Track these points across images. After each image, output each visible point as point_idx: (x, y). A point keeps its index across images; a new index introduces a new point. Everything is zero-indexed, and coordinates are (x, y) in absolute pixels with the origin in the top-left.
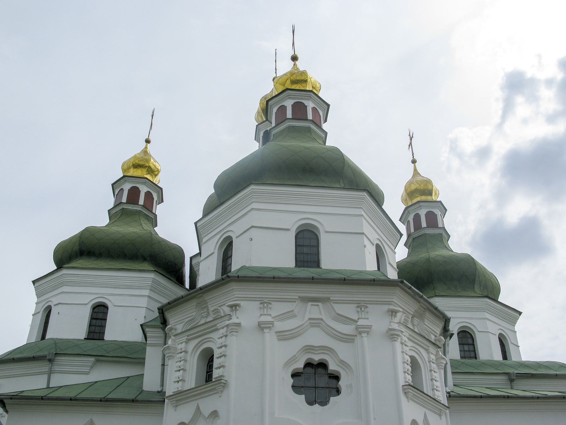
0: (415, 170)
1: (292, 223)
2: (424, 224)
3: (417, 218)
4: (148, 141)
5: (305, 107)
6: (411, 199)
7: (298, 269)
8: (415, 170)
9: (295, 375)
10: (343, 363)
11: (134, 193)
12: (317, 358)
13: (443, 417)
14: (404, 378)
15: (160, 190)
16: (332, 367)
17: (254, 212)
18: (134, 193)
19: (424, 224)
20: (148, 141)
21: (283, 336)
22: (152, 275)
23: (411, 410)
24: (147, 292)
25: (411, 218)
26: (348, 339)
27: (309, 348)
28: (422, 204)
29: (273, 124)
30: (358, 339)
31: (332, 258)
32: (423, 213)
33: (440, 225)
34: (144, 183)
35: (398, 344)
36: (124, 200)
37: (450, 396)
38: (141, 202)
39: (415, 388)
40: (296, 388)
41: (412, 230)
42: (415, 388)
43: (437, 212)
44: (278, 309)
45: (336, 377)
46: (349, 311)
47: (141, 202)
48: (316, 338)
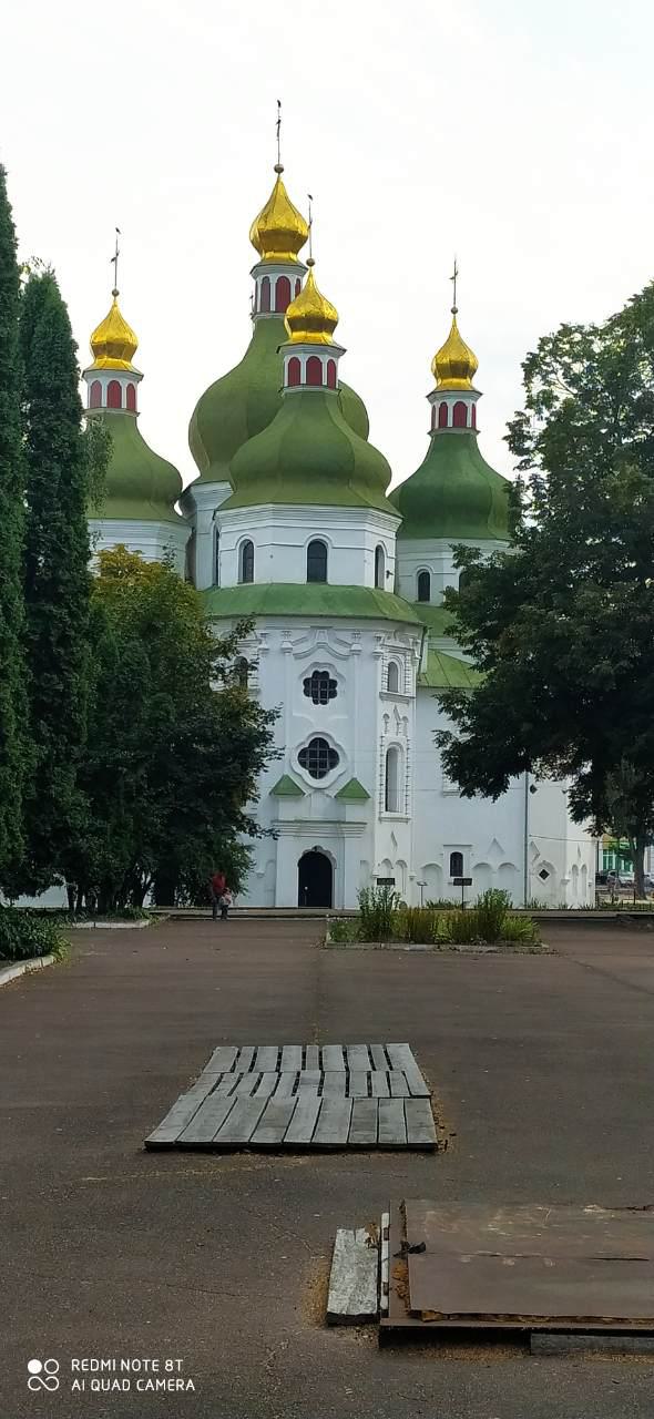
0: (454, 326)
1: (304, 539)
2: (450, 424)
3: (444, 407)
4: (115, 293)
6: (442, 379)
8: (454, 326)
9: (306, 682)
10: (339, 675)
11: (114, 388)
12: (321, 670)
13: (411, 705)
14: (381, 686)
15: (140, 377)
16: (331, 678)
18: (114, 388)
19: (450, 424)
20: (115, 293)
21: (298, 657)
22: (159, 524)
23: (386, 707)
24: (154, 541)
25: (438, 404)
26: (345, 658)
27: (316, 664)
28: (451, 393)
29: (286, 385)
30: (350, 660)
31: (337, 574)
32: (451, 403)
33: (469, 424)
34: (124, 377)
35: (380, 662)
36: (104, 404)
37: (418, 687)
38: (124, 405)
39: (391, 693)
40: (306, 693)
41: (437, 426)
42: (391, 693)
43: (469, 403)
44: (296, 635)
45: (334, 683)
46: (346, 636)
47: (124, 405)
48: (321, 657)
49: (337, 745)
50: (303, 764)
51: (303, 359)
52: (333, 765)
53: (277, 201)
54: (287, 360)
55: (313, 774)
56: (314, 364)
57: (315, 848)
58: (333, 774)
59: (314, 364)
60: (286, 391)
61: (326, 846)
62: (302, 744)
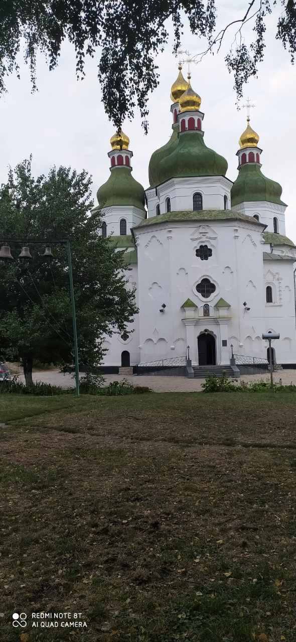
5: (194, 120)
7: (195, 212)
17: (176, 190)
29: (180, 131)
49: (214, 281)
50: (198, 291)
51: (187, 119)
52: (213, 291)
53: (180, 80)
54: (180, 120)
55: (203, 296)
56: (191, 121)
57: (206, 330)
58: (213, 295)
59: (191, 121)
60: (180, 134)
61: (212, 328)
62: (198, 281)
